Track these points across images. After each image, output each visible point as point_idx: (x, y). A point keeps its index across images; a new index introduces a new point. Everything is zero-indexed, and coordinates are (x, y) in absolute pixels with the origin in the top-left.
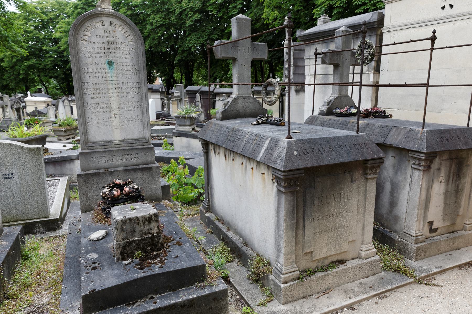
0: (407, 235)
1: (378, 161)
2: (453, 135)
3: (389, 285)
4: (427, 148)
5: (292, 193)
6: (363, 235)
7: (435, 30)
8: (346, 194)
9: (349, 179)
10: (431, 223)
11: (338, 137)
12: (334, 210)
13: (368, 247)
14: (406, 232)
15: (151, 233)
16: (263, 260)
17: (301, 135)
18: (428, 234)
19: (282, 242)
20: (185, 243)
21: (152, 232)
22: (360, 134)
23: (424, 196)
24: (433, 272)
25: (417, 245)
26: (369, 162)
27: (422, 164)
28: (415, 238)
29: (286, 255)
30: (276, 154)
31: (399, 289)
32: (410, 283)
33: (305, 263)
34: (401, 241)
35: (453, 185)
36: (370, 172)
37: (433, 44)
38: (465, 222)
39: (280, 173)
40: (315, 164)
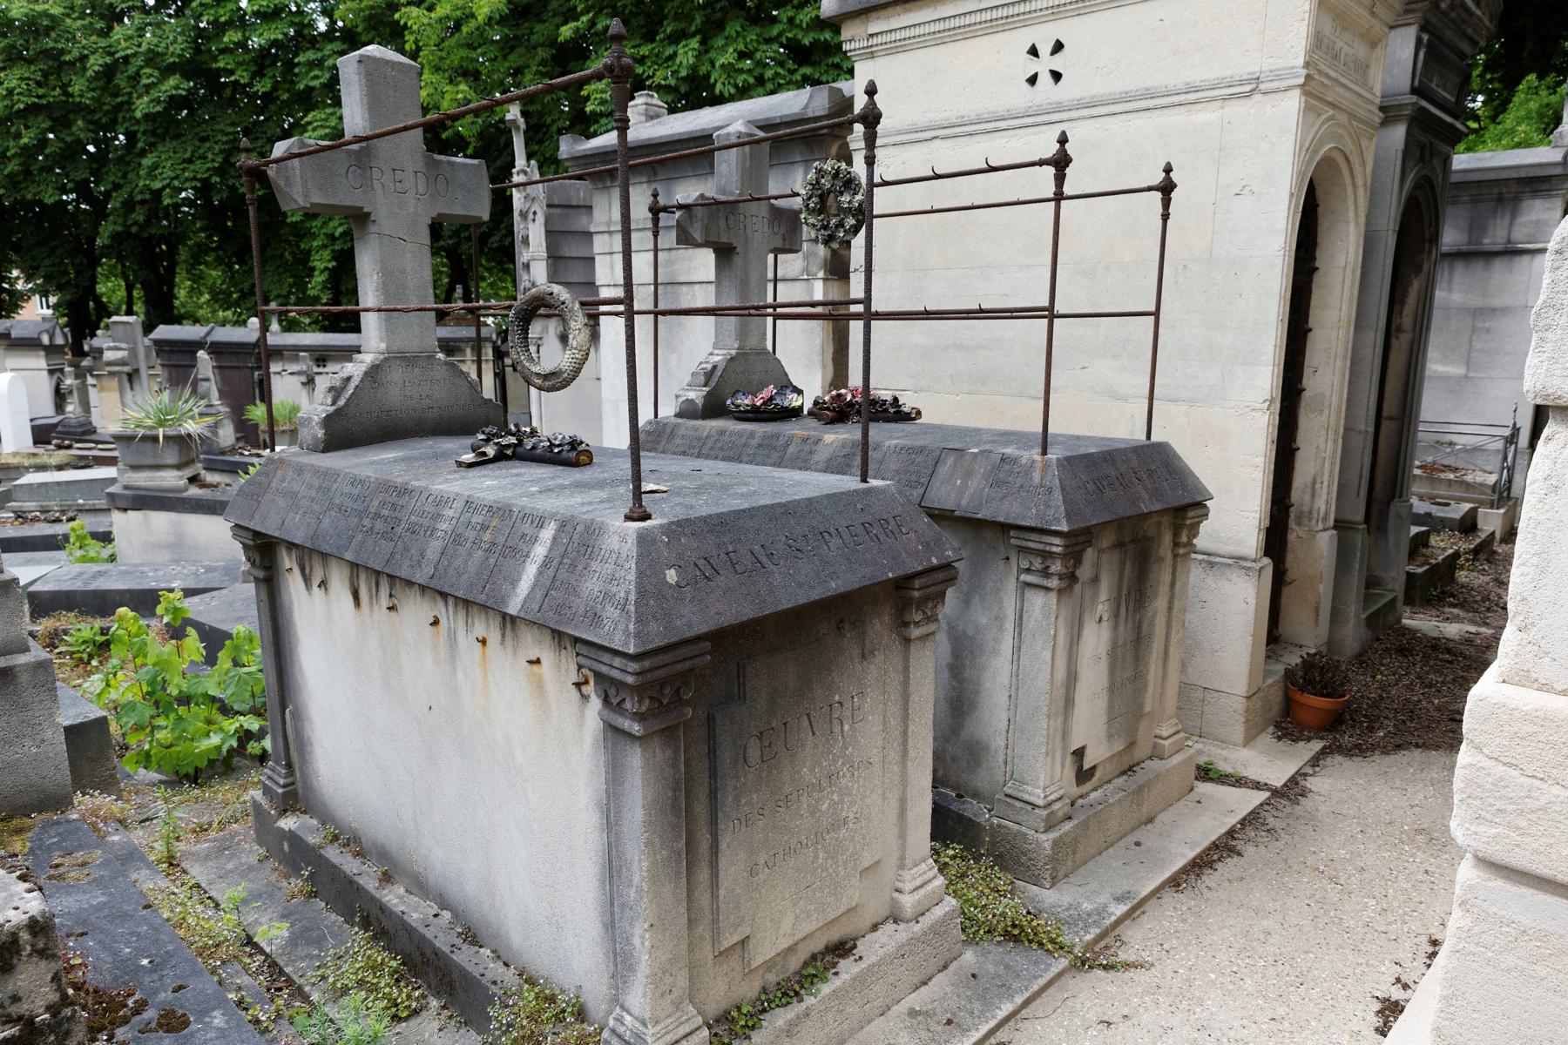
0: (1017, 804)
1: (941, 575)
2: (1123, 469)
3: (1001, 997)
4: (1068, 516)
5: (668, 734)
6: (902, 836)
7: (1064, 133)
8: (848, 705)
9: (856, 651)
10: (1079, 754)
11: (810, 501)
12: (812, 770)
13: (921, 880)
14: (1014, 793)
15: (20, 1018)
16: (552, 999)
17: (677, 500)
18: (1075, 791)
19: (638, 931)
20: (204, 1013)
21: (23, 1008)
22: (874, 483)
23: (1061, 674)
24: (1113, 918)
25: (1053, 835)
26: (917, 583)
27: (1053, 569)
28: (1044, 813)
29: (655, 980)
30: (591, 586)
31: (1033, 1006)
32: (1060, 975)
33: (722, 990)
34: (999, 826)
35: (1130, 624)
36: (918, 617)
37: (1060, 179)
38: (1158, 732)
39: (617, 662)
40: (748, 611)
